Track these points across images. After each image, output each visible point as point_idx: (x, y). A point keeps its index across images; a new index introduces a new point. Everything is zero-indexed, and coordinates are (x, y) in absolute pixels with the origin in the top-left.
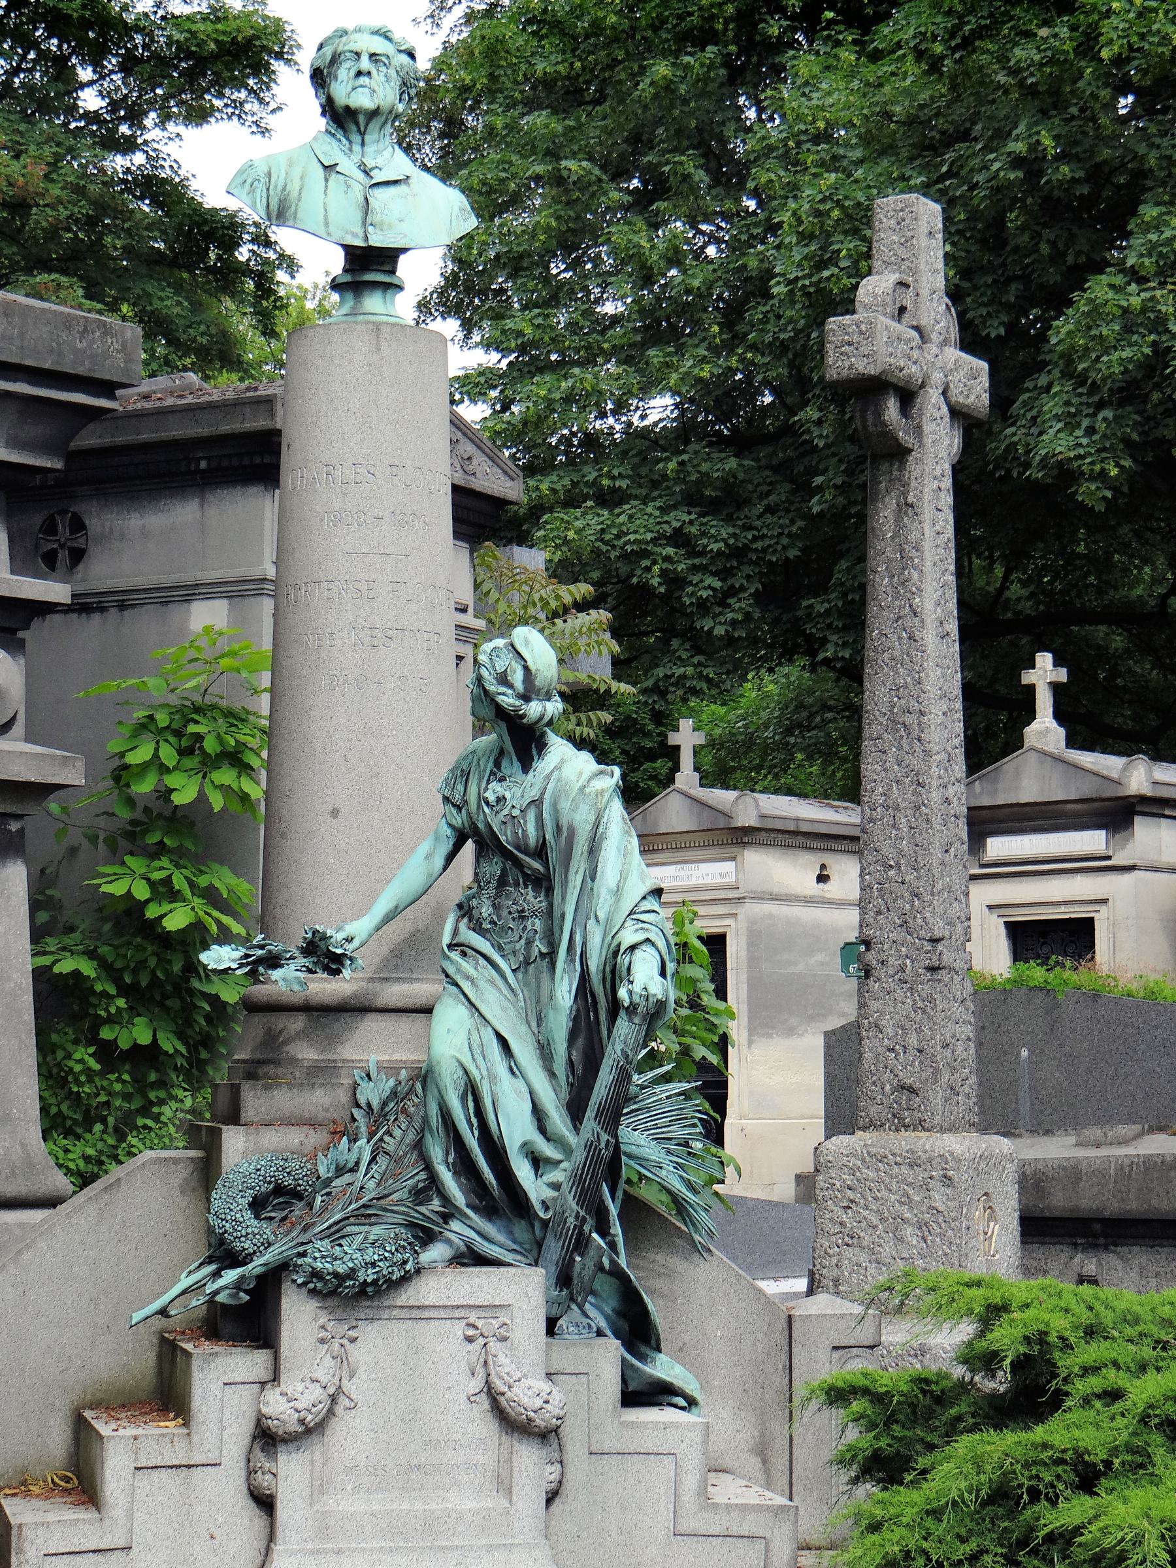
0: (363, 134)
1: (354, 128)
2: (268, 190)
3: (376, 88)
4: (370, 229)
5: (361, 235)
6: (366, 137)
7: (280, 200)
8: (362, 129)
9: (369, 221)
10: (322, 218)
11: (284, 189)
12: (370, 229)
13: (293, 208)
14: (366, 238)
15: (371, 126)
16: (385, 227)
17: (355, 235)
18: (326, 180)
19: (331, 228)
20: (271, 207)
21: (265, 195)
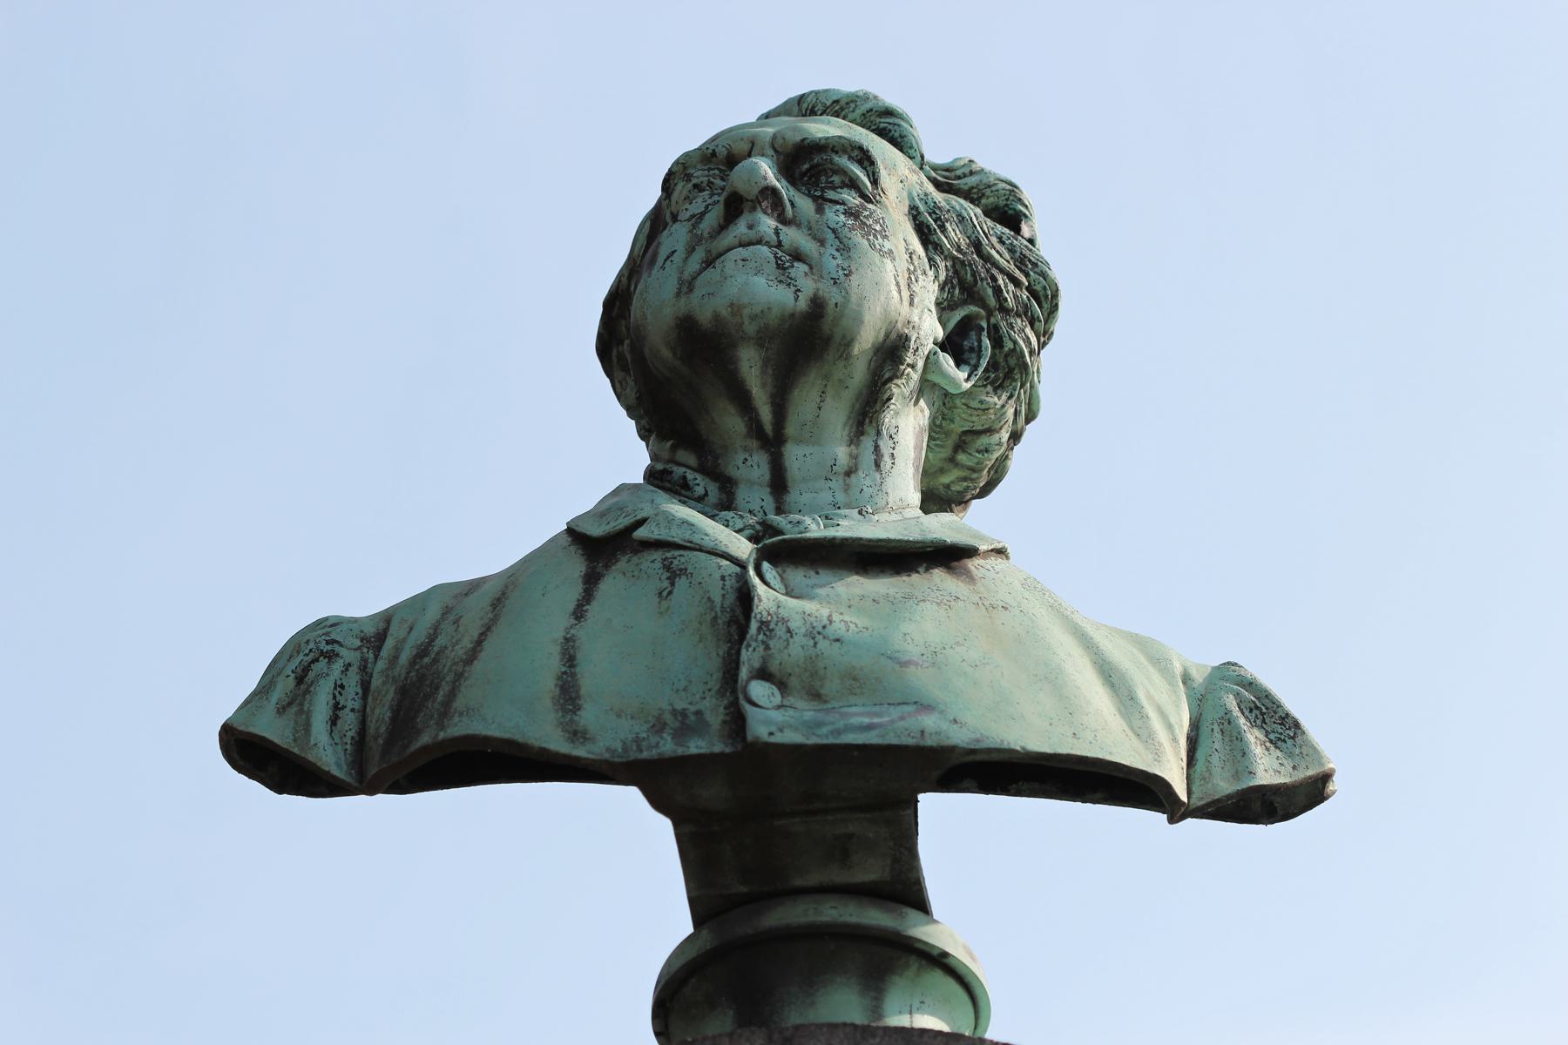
0: (773, 442)
1: (732, 423)
2: (365, 686)
3: (808, 245)
4: (760, 690)
5: (716, 718)
6: (796, 457)
7: (403, 692)
8: (766, 414)
9: (750, 658)
10: (547, 683)
11: (423, 651)
12: (760, 690)
13: (445, 689)
14: (737, 722)
15: (805, 400)
16: (831, 687)
17: (687, 725)
18: (591, 581)
19: (589, 716)
20: (371, 730)
21: (351, 698)
